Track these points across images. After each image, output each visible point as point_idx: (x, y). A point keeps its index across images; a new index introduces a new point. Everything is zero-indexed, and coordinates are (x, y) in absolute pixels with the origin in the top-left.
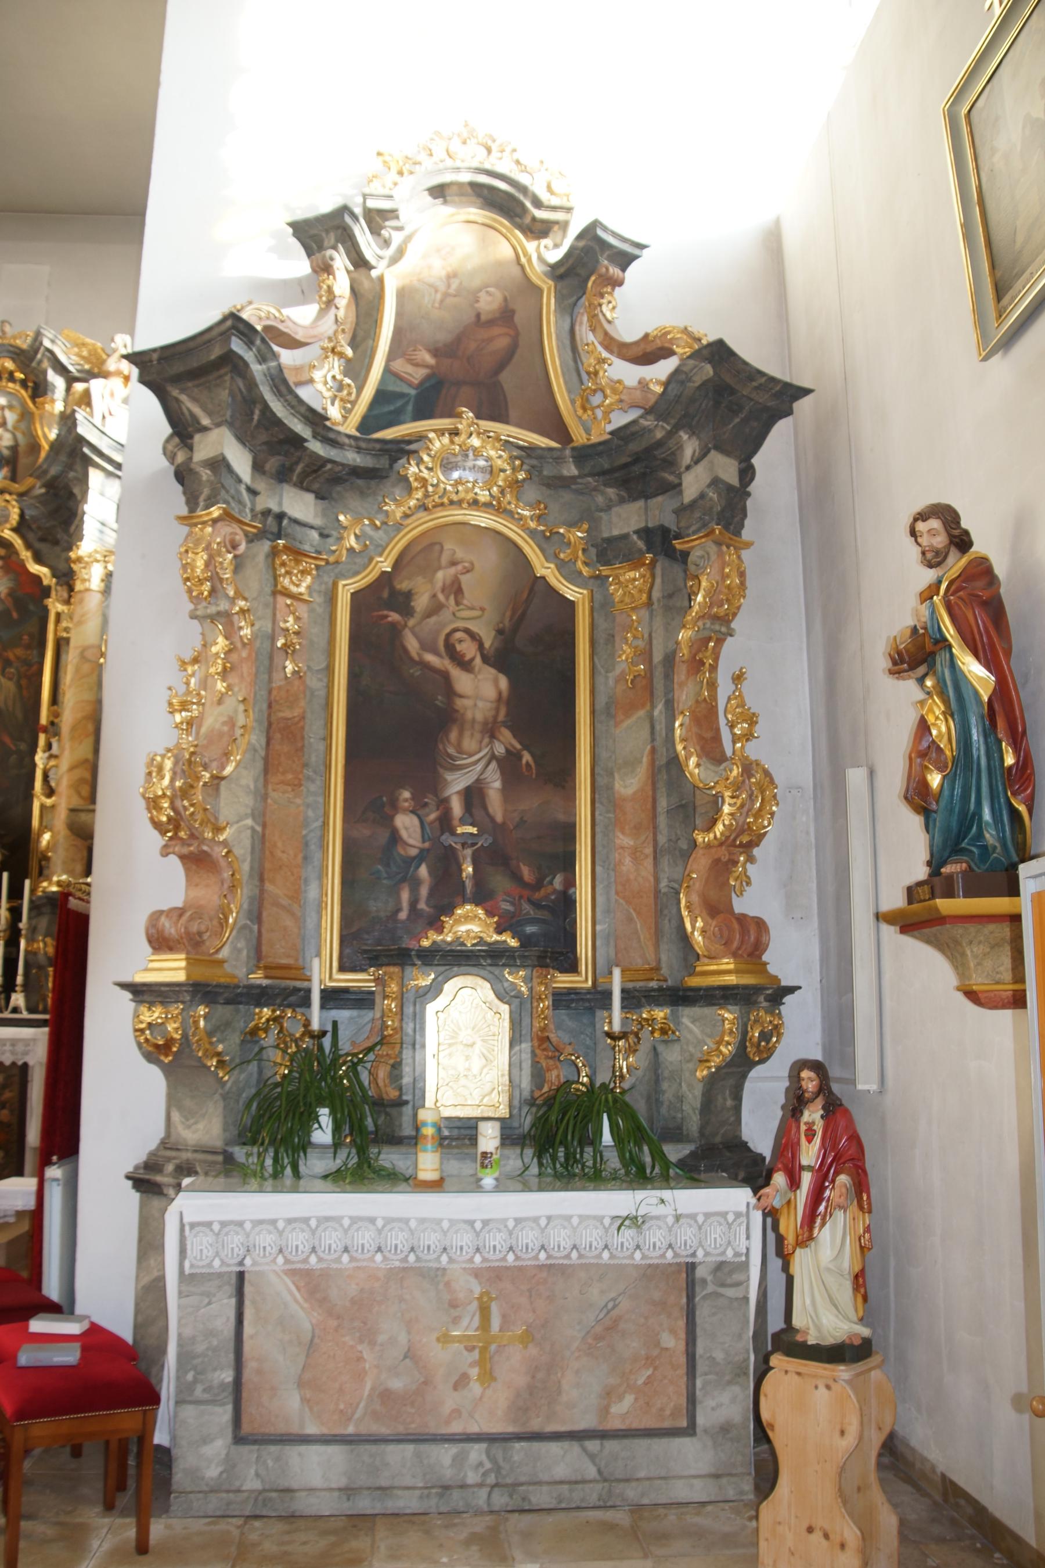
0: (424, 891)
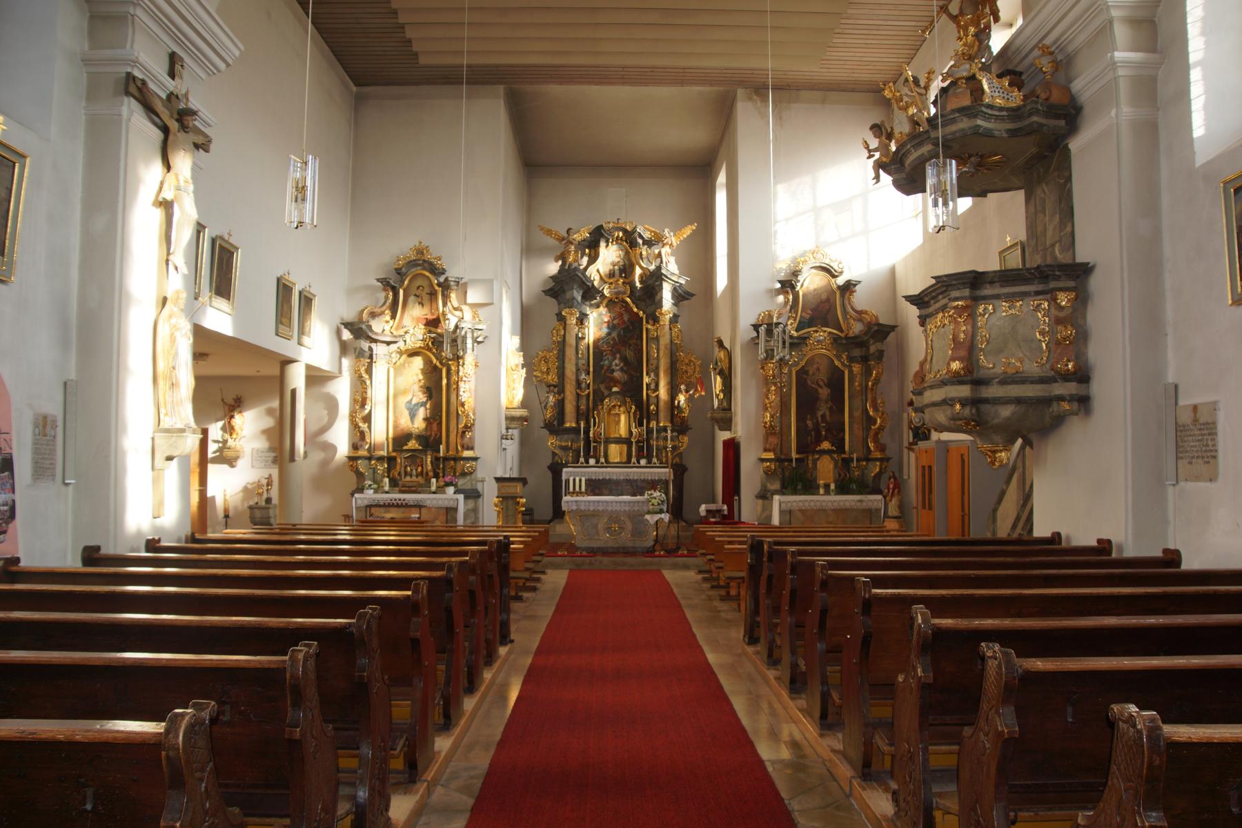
0: (813, 437)
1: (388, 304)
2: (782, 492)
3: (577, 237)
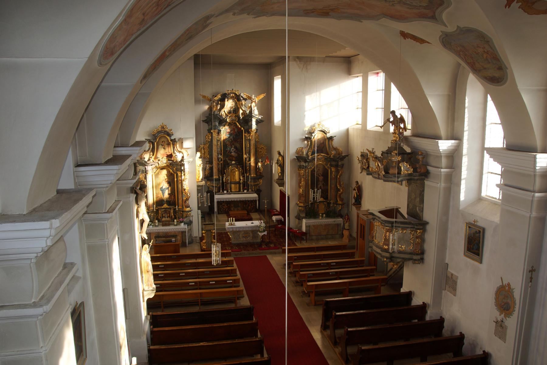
1: (151, 149)
2: (305, 218)
3: (216, 98)
